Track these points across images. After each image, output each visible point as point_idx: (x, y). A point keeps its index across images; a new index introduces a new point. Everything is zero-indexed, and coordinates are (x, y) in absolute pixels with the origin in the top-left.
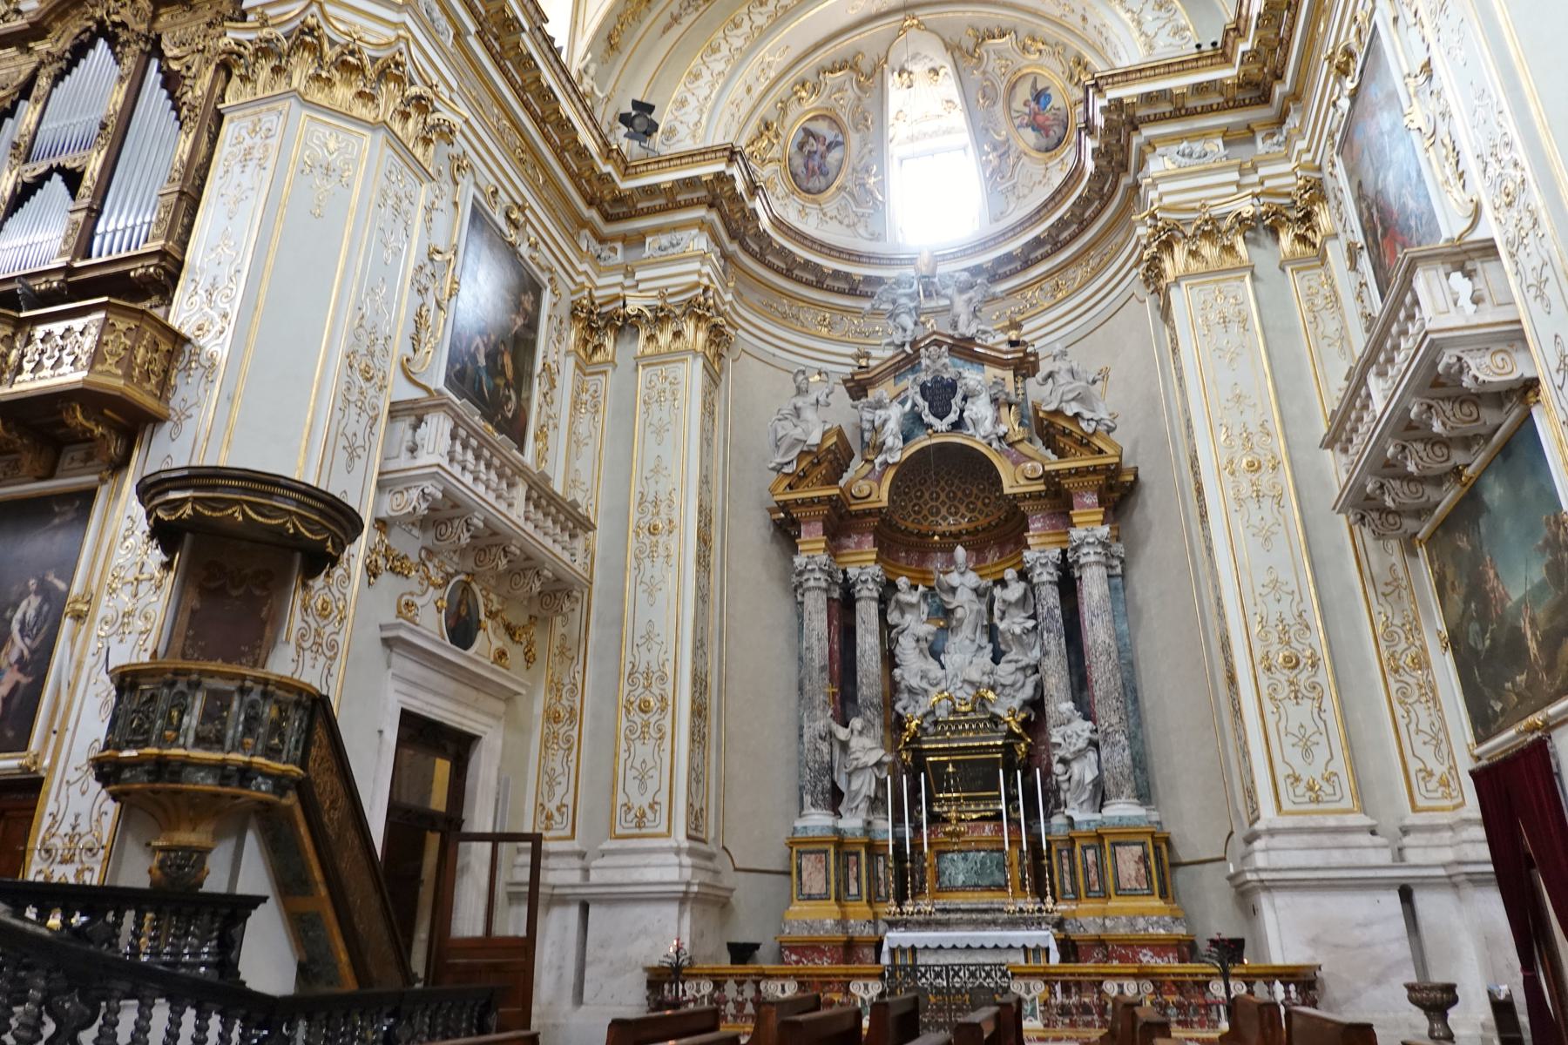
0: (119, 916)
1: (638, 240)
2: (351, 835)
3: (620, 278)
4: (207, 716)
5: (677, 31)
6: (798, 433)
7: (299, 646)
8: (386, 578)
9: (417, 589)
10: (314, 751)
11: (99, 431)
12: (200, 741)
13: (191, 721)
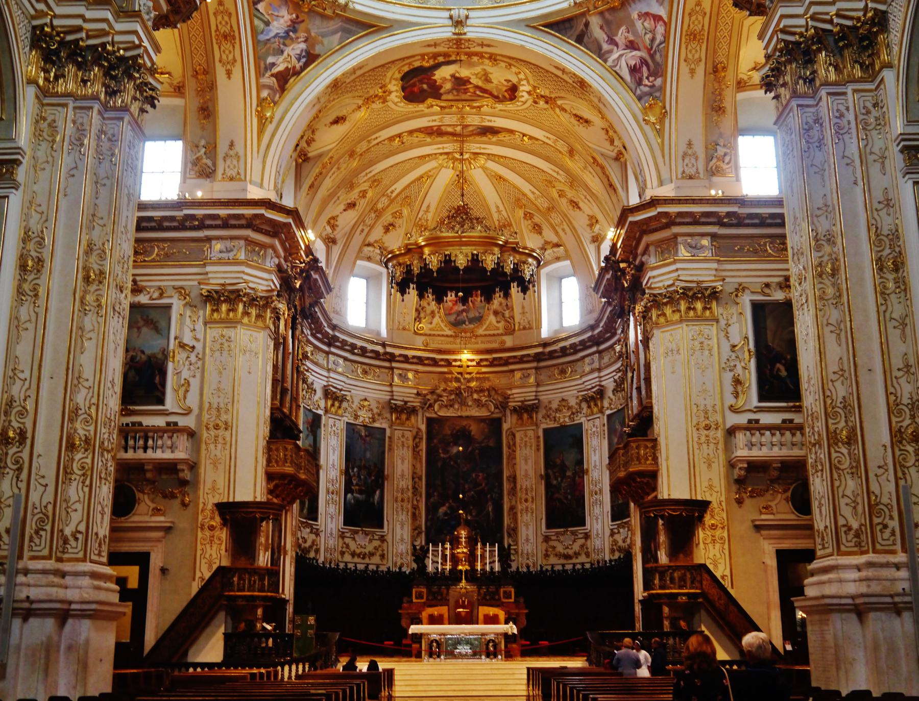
2: (732, 607)
4: (660, 580)
8: (748, 502)
9: (770, 498)
10: (704, 583)
11: (645, 480)
12: (662, 588)
13: (657, 582)
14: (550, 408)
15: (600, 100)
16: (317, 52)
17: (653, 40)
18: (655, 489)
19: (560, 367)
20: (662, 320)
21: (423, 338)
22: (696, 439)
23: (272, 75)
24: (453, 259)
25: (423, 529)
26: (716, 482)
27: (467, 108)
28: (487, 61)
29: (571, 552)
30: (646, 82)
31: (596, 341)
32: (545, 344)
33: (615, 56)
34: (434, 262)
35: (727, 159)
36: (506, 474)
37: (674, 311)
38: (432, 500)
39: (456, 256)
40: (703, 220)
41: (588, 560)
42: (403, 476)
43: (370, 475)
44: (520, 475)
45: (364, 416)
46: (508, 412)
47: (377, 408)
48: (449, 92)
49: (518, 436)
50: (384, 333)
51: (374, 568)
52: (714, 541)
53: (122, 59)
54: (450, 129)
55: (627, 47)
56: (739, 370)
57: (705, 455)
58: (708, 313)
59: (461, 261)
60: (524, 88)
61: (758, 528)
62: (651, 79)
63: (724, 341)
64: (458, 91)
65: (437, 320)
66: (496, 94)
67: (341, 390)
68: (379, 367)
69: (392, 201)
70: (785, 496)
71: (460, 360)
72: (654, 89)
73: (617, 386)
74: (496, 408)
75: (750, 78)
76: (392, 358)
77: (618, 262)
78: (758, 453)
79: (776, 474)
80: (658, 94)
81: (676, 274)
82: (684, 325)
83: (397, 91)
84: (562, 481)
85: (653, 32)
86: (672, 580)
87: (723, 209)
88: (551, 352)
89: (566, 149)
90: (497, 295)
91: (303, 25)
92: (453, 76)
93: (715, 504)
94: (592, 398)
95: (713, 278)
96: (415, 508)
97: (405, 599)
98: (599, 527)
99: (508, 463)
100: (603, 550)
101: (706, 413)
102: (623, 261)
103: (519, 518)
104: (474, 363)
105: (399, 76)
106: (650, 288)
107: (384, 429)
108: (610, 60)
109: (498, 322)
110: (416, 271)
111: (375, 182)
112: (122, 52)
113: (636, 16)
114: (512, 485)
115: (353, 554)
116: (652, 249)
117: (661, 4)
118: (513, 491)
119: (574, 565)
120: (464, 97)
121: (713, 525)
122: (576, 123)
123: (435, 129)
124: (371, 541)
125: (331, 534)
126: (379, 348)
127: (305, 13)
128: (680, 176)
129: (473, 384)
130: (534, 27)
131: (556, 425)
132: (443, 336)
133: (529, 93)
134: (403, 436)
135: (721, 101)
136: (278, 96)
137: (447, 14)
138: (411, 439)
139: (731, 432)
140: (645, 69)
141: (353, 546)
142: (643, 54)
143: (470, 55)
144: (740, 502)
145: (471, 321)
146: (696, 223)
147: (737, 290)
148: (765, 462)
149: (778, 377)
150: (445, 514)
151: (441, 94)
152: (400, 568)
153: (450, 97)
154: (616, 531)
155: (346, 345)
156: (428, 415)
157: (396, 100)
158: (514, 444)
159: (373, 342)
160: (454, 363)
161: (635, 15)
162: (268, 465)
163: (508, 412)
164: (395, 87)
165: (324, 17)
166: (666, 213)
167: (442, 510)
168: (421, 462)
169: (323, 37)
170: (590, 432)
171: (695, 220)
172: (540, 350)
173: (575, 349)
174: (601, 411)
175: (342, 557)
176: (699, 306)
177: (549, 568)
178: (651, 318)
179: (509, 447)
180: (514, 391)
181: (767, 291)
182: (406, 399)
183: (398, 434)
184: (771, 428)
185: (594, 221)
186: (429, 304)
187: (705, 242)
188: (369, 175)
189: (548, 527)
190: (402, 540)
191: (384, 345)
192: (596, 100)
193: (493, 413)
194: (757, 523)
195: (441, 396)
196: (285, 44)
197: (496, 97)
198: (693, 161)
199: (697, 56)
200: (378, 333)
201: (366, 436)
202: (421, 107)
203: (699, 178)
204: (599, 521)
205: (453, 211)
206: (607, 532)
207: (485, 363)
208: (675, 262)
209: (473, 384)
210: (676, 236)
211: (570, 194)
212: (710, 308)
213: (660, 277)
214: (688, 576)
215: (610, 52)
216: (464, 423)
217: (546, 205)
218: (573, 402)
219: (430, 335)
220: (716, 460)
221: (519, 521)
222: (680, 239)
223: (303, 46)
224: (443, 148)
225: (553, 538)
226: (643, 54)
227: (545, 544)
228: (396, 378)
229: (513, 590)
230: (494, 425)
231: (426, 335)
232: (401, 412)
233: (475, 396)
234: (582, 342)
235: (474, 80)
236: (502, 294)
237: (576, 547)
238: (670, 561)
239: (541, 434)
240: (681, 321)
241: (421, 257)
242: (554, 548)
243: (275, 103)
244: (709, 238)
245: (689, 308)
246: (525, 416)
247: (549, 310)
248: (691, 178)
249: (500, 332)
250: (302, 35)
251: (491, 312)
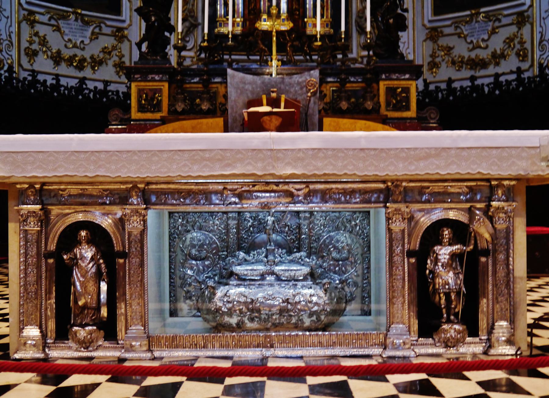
29: (484, 54)
51: (100, 86)
115: (57, 59)
119: (497, 76)
124: (95, 36)
141: (55, 42)
177: (443, 86)
189: (437, 10)
225: (447, 31)
227: (430, 44)
237: (497, 44)
242: (449, 49)
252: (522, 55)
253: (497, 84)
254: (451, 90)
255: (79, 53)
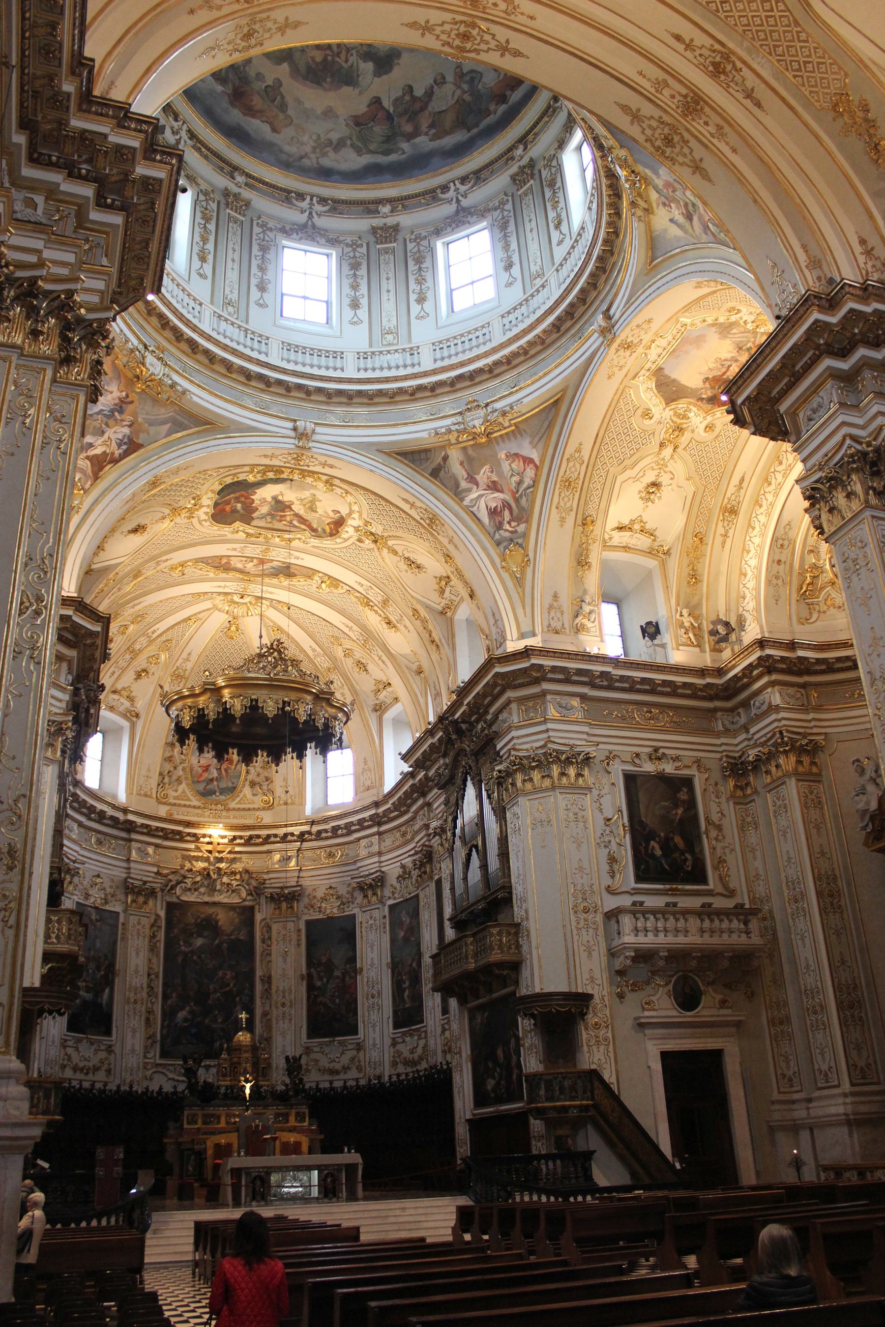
0: (539, 1163)
1: (745, 704)
3: (744, 736)
4: (547, 1090)
5: (729, 541)
6: (861, 806)
7: (588, 1046)
8: (630, 996)
10: (596, 1092)
11: (505, 973)
12: (548, 1099)
13: (542, 1092)
14: (314, 897)
15: (451, 541)
16: (140, 441)
17: (520, 483)
18: (517, 983)
19: (328, 850)
20: (528, 786)
21: (167, 808)
22: (574, 924)
23: (87, 458)
24: (260, 705)
25: (159, 1037)
26: (597, 974)
27: (277, 540)
28: (320, 485)
29: (338, 1066)
30: (507, 527)
31: (377, 821)
32: (313, 823)
33: (474, 495)
34: (237, 707)
35: (593, 617)
36: (259, 973)
37: (543, 777)
38: (169, 1002)
39: (265, 701)
40: (575, 678)
41: (361, 1075)
42: (136, 971)
43: (98, 968)
44: (276, 974)
45: (96, 897)
46: (263, 900)
47: (111, 887)
48: (263, 517)
49: (275, 927)
50: (122, 797)
52: (598, 1043)
53: (80, 320)
54: (239, 566)
55: (489, 488)
56: (614, 847)
57: (585, 942)
58: (581, 779)
59: (270, 708)
60: (354, 522)
61: (641, 1026)
62: (513, 524)
63: (597, 812)
64: (273, 516)
65: (183, 787)
66: (315, 526)
67: (74, 862)
68: (116, 837)
69: (151, 642)
70: (666, 989)
71: (210, 836)
72: (514, 536)
73: (405, 872)
74: (248, 894)
75: (610, 538)
76: (130, 827)
77: (456, 722)
78: (647, 940)
79: (661, 963)
80: (520, 541)
81: (545, 735)
82: (558, 791)
83: (208, 506)
84: (328, 982)
85: (521, 474)
86: (562, 1090)
87: (598, 668)
88: (319, 832)
89: (380, 599)
90: (289, 756)
91: (130, 408)
92: (275, 498)
93: (597, 999)
94: (370, 886)
95: (584, 743)
96: (150, 1012)
97: (171, 1124)
98: (377, 1035)
99: (261, 960)
100: (381, 1063)
101: (584, 894)
102: (464, 722)
103: (274, 1026)
104: (226, 841)
105: (218, 487)
106: (514, 749)
107: (118, 913)
108: (467, 502)
109: (254, 795)
110: (212, 716)
111: (138, 618)
112: (83, 311)
113: (503, 456)
114: (266, 986)
115: (75, 1069)
116: (514, 706)
117: (534, 447)
118: (267, 993)
120: (277, 525)
121: (596, 1024)
122: (405, 567)
123: (224, 561)
125: (53, 1042)
126: (121, 816)
127: (137, 393)
128: (546, 629)
129: (222, 865)
130: (385, 453)
131: (321, 916)
132: (189, 806)
133: (357, 529)
134: (139, 923)
135: (587, 556)
136: (89, 483)
137: (290, 425)
138: (148, 927)
139: (612, 915)
140: (507, 513)
142: (507, 497)
143: (305, 473)
144: (621, 996)
145: (223, 791)
146: (567, 681)
147: (608, 758)
148: (650, 950)
149: (653, 856)
150: (185, 1020)
151: (253, 519)
152: (131, 1087)
153: (262, 523)
154: (400, 1040)
155: (84, 807)
156: (169, 899)
157: (203, 517)
158: (270, 938)
159: (114, 807)
160: (202, 840)
161: (502, 455)
162: (46, 942)
163: (263, 900)
164: (208, 501)
165: (155, 401)
166: (541, 666)
167: (182, 1015)
168: (158, 956)
169: (151, 425)
170: (364, 925)
171: (567, 677)
172: (306, 828)
173: (349, 829)
174: (381, 901)
175: (63, 1072)
176: (572, 771)
177: (314, 1085)
178: (513, 784)
179: (263, 941)
180: (271, 876)
181: (637, 761)
182: (145, 879)
183: (133, 920)
184: (654, 912)
185: (381, 687)
186: (175, 768)
187: (575, 702)
188: (137, 608)
189: (309, 1036)
190: (133, 1051)
191: (125, 811)
192: (445, 541)
193: (244, 900)
194: (643, 1020)
195: (185, 877)
196: (107, 425)
197: (314, 530)
198: (559, 615)
199: (568, 505)
200: (115, 797)
201: (97, 920)
202: (226, 531)
203: (565, 633)
204: (377, 1029)
205: (265, 650)
206: (388, 1041)
207: (238, 841)
208: (545, 721)
209: (222, 865)
210: (544, 693)
211: (359, 654)
212: (582, 776)
213: (521, 737)
214: (580, 1083)
215: (469, 490)
216: (211, 910)
217: (326, 665)
218: (343, 891)
219: (175, 805)
220: (596, 948)
221: (274, 1030)
222: (549, 697)
223: (127, 431)
224: (225, 587)
225: (316, 1049)
226: (507, 497)
228: (134, 853)
229: (307, 1111)
230: (247, 914)
231: (170, 804)
232: (139, 893)
233: (225, 879)
234: (361, 822)
235: (297, 508)
236: (295, 755)
237: (345, 1060)
238: (545, 1068)
239: (302, 926)
240: (553, 788)
241: (219, 701)
242: (317, 1061)
243: (86, 491)
244: (578, 699)
245: (563, 774)
246: (284, 905)
247: (313, 785)
248: (557, 633)
249: (256, 806)
250: (128, 418)
251: (247, 783)
252: (359, 1069)
253: (345, 1087)
254: (318, 1089)
255: (86, 1063)
